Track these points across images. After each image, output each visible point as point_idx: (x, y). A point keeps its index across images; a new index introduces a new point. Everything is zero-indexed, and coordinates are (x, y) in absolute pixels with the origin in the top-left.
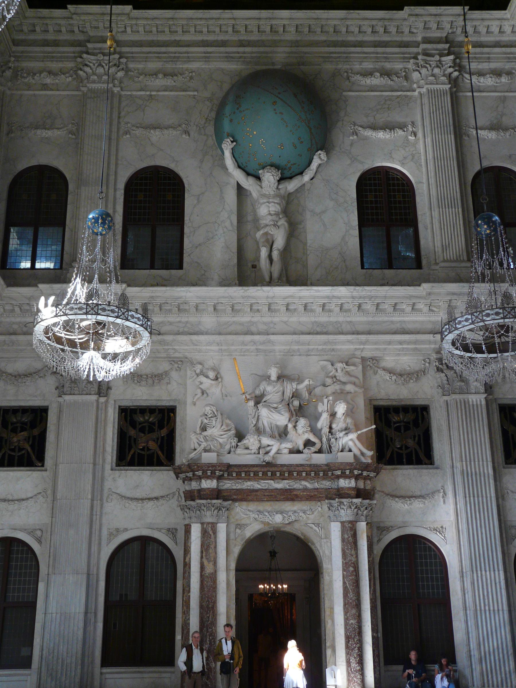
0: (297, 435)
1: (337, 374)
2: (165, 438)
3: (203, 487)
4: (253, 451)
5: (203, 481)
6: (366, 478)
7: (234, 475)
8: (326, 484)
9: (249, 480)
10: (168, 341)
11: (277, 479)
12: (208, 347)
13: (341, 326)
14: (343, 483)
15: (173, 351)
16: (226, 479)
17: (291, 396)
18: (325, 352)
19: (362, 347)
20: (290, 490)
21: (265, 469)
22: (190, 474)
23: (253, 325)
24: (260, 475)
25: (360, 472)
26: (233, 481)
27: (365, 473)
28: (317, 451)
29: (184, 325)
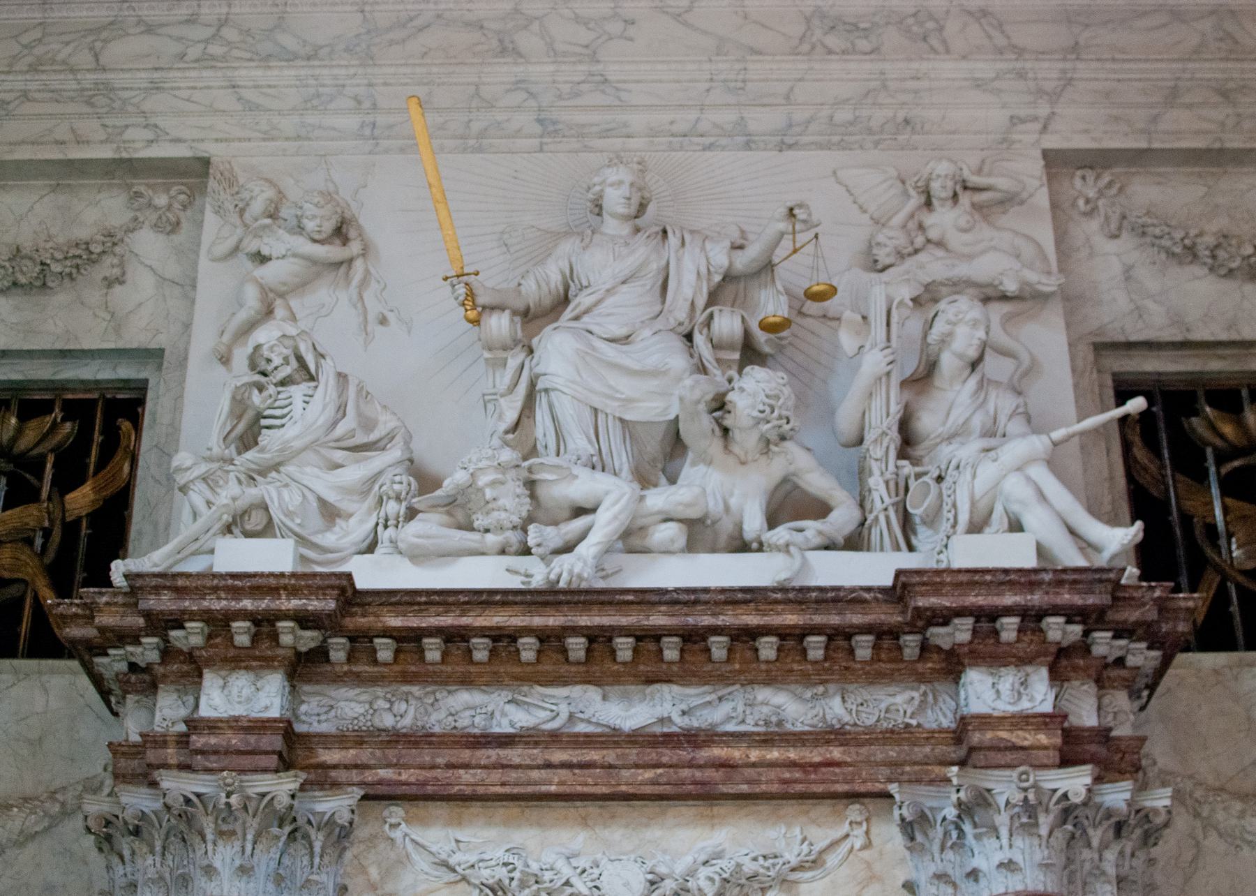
0: (731, 460)
1: (929, 219)
2: (84, 531)
3: (205, 712)
4: (492, 539)
5: (211, 680)
6: (1106, 675)
7: (385, 655)
8: (894, 703)
9: (466, 682)
10: (126, 94)
11: (616, 679)
12: (311, 119)
13: (941, 29)
14: (985, 692)
15: (149, 135)
16: (338, 679)
17: (701, 301)
18: (870, 131)
19: (1043, 110)
20: (693, 739)
21: (552, 620)
22: (147, 651)
23: (526, 27)
24: (528, 655)
25: (1076, 629)
26: (379, 691)
27: (1103, 644)
28: (841, 540)
29: (210, 32)
